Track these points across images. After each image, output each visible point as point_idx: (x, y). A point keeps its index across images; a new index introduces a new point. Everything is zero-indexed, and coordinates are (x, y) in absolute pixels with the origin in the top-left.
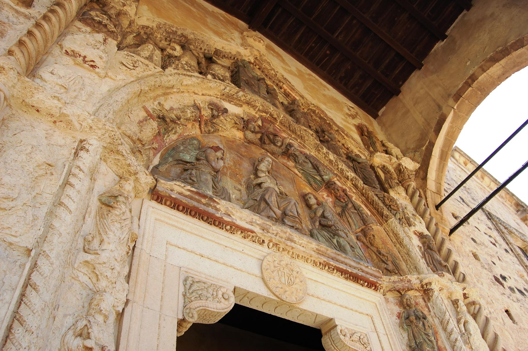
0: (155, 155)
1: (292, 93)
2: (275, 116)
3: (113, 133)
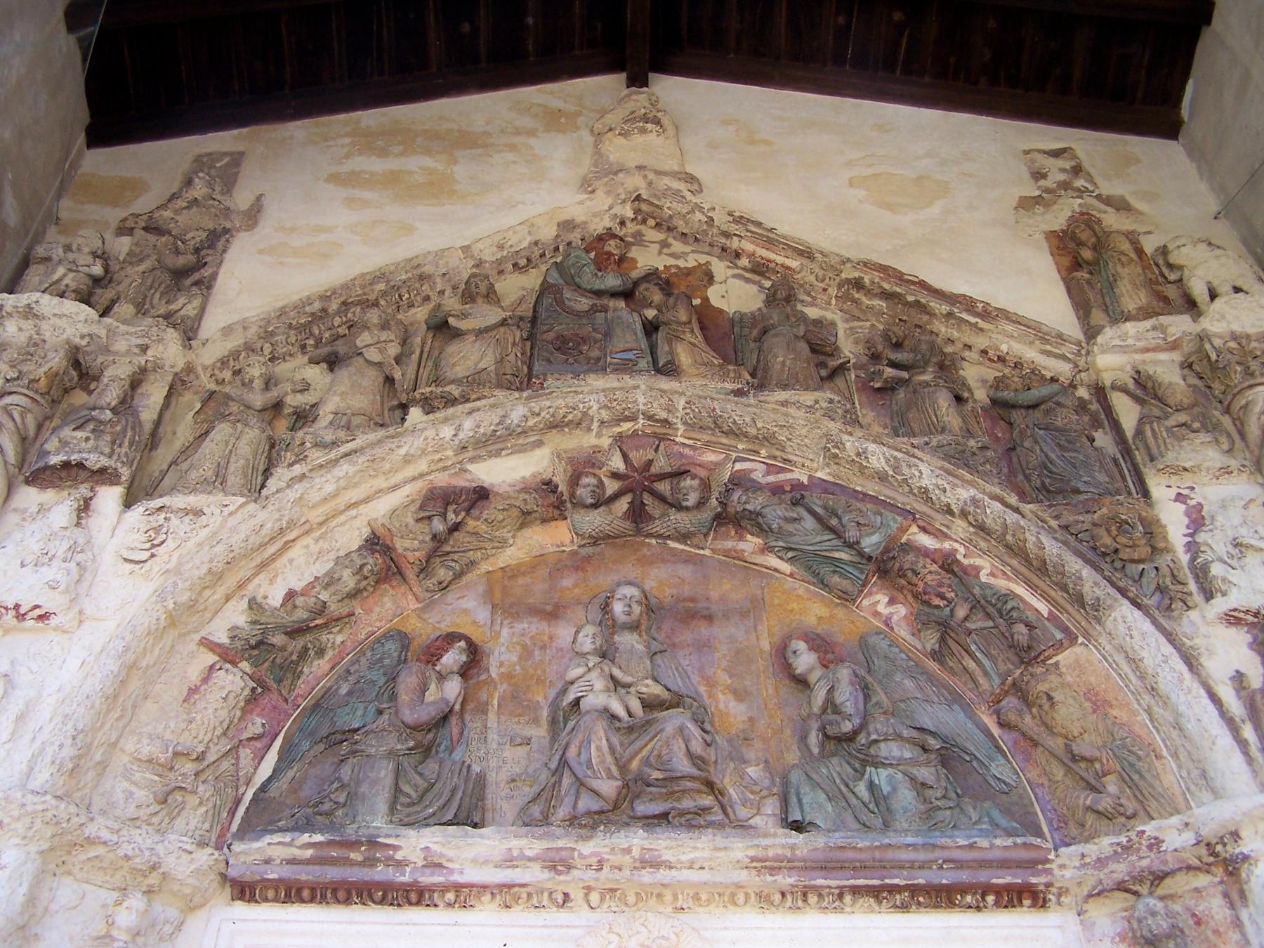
0: (260, 757)
1: (772, 256)
2: (664, 415)
3: (49, 814)
